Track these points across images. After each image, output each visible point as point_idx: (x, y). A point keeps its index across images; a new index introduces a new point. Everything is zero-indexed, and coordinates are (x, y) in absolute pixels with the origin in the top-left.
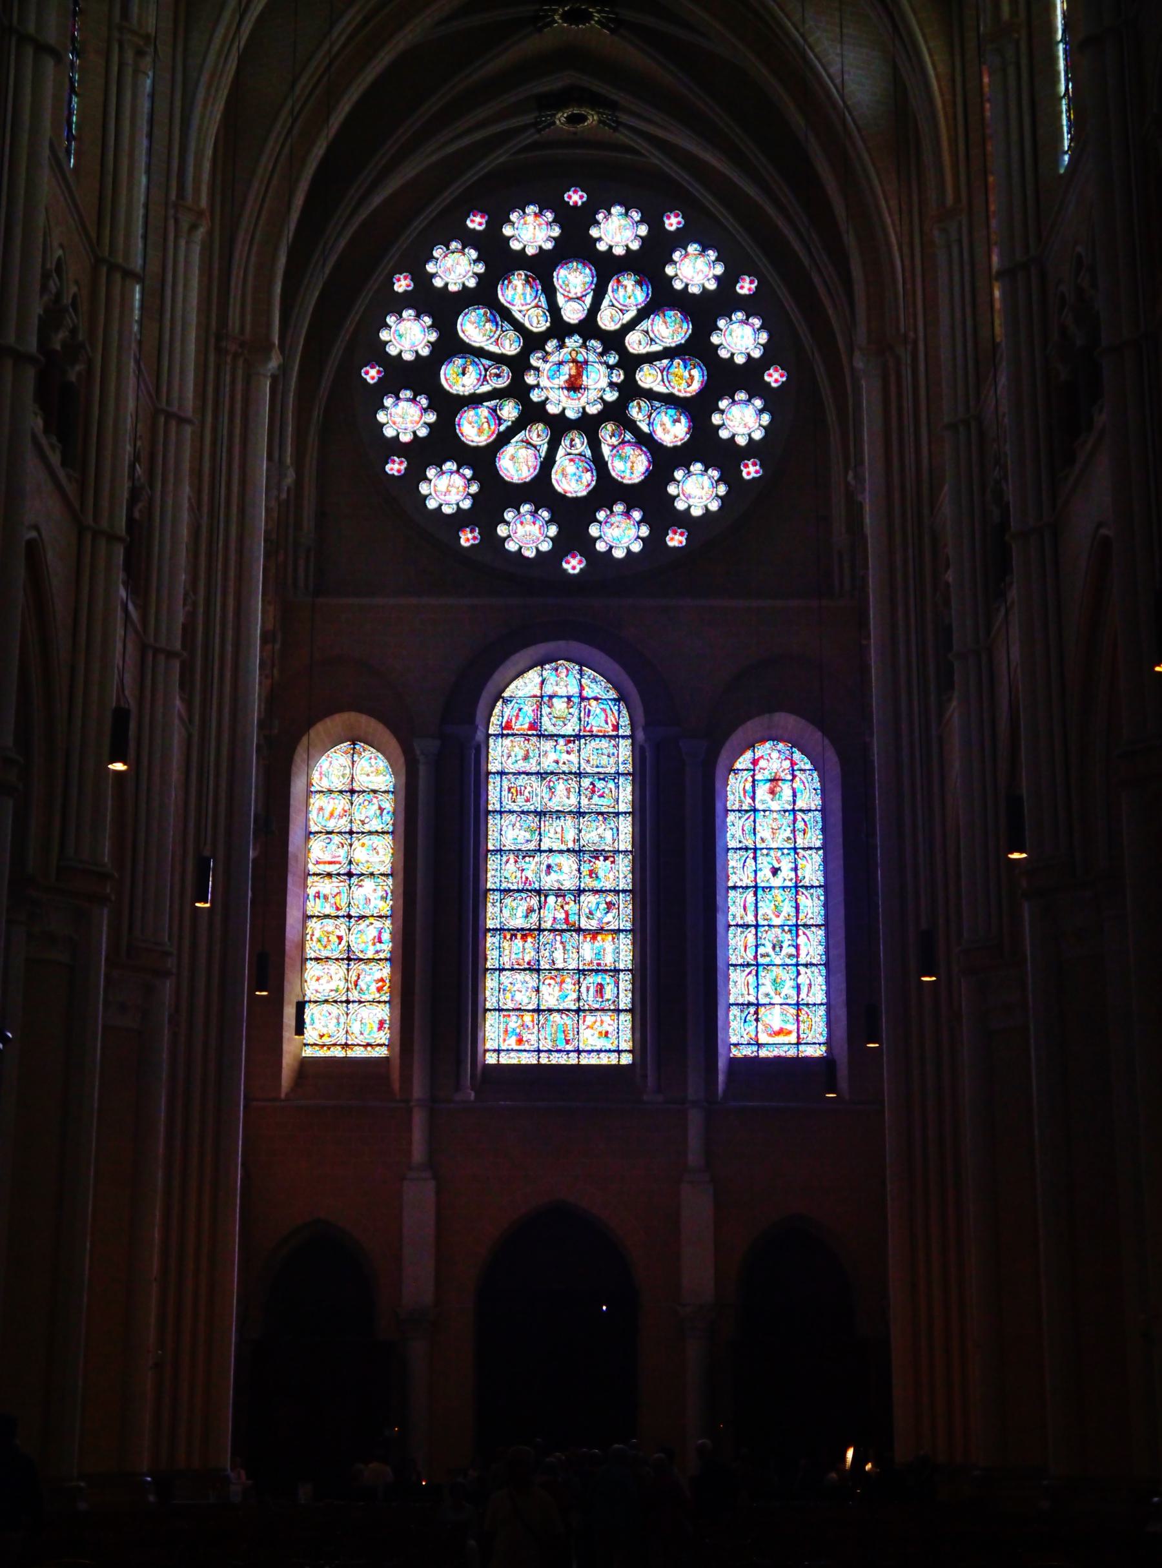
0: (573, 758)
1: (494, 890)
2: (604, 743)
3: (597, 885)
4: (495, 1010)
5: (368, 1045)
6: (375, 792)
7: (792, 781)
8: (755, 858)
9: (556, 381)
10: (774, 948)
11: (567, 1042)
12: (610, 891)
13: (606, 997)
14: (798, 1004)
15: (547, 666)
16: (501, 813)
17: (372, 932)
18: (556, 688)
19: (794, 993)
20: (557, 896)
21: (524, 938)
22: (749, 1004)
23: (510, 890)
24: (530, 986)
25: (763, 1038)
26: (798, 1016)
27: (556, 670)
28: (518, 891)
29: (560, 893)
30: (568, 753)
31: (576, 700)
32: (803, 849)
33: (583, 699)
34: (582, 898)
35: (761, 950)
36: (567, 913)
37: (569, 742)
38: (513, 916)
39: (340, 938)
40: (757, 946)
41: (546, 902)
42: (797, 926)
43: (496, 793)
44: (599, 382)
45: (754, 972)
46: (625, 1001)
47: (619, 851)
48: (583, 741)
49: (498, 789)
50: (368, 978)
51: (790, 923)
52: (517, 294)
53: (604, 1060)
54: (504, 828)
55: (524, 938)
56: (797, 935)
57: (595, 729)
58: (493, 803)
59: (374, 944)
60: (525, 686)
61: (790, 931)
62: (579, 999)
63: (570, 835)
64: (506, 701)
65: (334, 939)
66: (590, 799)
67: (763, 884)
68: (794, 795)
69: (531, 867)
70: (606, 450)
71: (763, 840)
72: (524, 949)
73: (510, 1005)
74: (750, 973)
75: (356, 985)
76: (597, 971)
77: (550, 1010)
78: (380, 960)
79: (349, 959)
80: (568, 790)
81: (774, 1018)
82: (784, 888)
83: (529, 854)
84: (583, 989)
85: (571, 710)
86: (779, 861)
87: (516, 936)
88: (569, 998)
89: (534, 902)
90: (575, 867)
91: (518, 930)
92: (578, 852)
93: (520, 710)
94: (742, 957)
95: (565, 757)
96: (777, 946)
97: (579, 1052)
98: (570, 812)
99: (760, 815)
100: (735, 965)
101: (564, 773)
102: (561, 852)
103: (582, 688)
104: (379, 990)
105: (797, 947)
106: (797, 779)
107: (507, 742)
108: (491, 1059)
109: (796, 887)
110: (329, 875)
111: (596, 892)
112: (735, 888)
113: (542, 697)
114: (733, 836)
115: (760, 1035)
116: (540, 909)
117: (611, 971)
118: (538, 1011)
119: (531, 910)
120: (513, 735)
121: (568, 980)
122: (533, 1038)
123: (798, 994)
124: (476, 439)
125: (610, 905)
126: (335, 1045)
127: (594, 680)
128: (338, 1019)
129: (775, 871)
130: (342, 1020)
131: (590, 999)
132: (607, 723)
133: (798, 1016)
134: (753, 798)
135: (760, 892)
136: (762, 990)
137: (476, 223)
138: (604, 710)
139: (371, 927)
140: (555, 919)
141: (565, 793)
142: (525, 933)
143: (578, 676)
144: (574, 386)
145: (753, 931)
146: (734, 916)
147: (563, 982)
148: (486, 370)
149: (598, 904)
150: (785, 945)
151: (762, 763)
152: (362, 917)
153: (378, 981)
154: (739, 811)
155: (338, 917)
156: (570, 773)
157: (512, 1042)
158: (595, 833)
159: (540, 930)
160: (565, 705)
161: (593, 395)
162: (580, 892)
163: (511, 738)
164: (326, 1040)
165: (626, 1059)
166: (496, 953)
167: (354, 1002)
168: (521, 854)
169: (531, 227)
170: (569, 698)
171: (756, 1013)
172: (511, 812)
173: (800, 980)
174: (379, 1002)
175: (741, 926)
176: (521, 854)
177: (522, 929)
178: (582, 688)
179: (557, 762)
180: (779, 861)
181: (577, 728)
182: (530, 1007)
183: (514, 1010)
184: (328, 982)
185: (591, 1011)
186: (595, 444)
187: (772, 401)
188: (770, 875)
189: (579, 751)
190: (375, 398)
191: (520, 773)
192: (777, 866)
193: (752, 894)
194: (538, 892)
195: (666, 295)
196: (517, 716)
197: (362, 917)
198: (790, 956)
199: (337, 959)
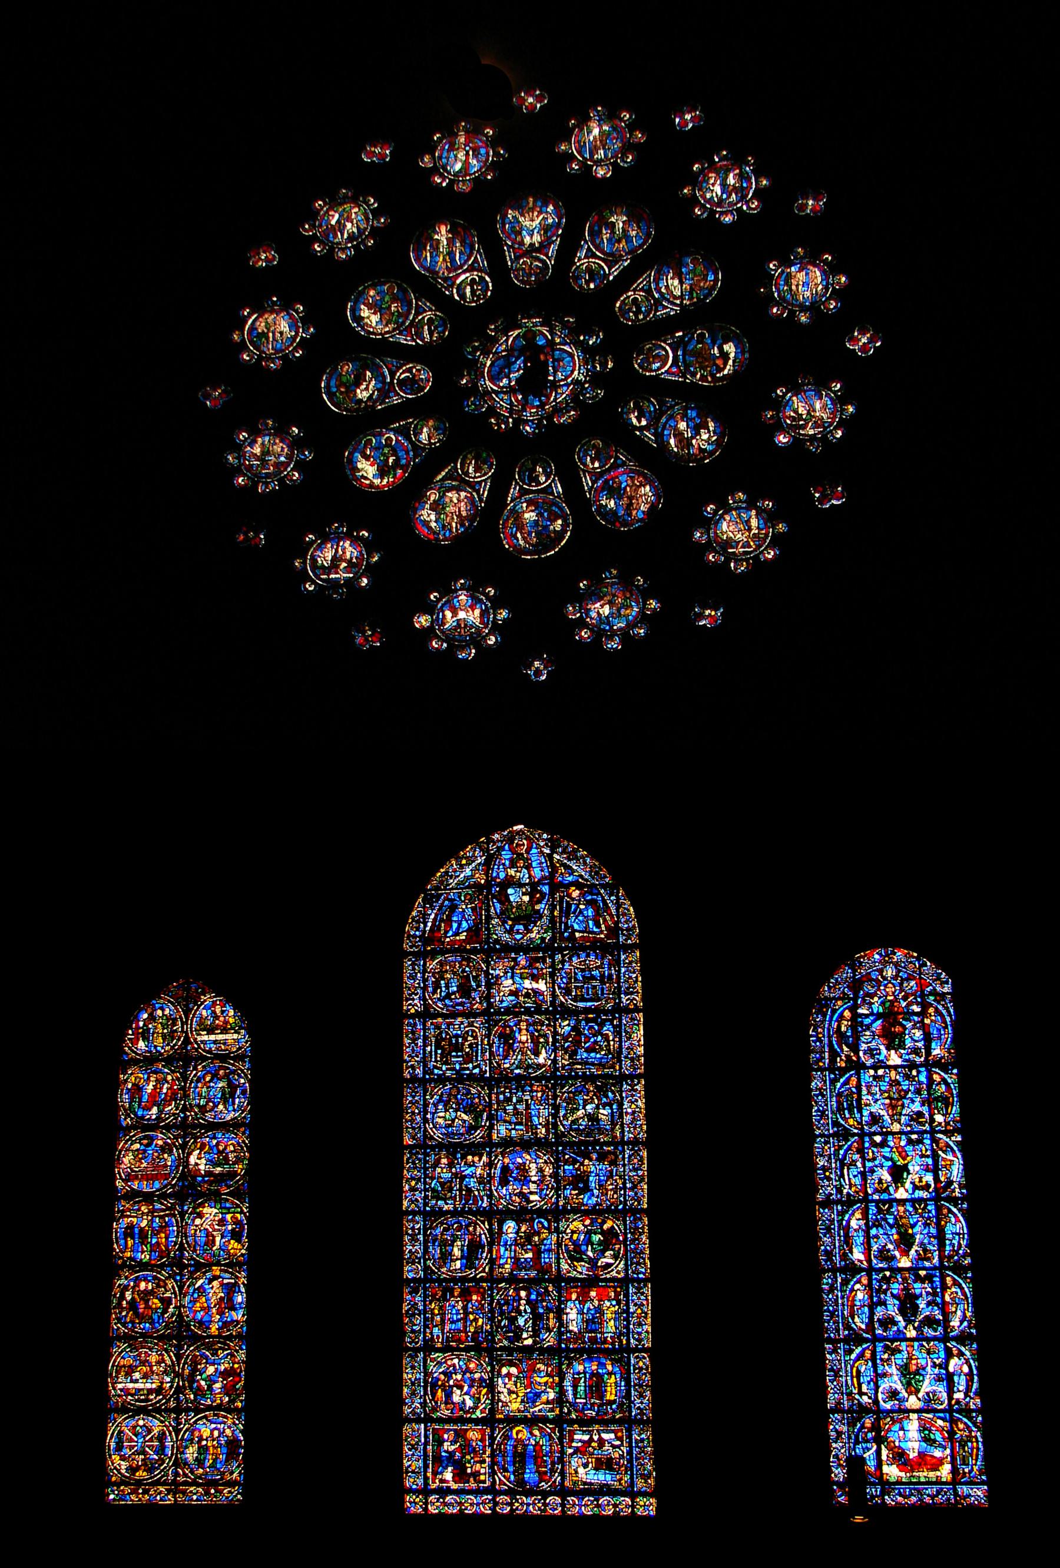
0: (541, 986)
1: (414, 1213)
2: (593, 960)
3: (589, 1201)
4: (418, 1421)
5: (214, 1483)
6: (224, 1058)
7: (923, 1014)
8: (861, 1151)
9: (505, 381)
10: (902, 1311)
11: (542, 1476)
12: (608, 1210)
13: (610, 1397)
14: (950, 1410)
15: (496, 836)
16: (423, 1082)
17: (215, 1292)
18: (511, 872)
19: (941, 1389)
20: (519, 1222)
21: (465, 1295)
22: (863, 1410)
23: (441, 1213)
24: (477, 1376)
25: (892, 1472)
26: (952, 1433)
27: (510, 840)
28: (455, 1213)
29: (521, 1215)
30: (535, 978)
31: (546, 889)
32: (945, 1132)
33: (555, 887)
34: (562, 1225)
35: (879, 1312)
36: (538, 1253)
37: (537, 960)
38: (446, 1257)
39: (166, 1302)
40: (872, 1307)
41: (500, 1232)
42: (941, 1267)
43: (415, 1052)
44: (571, 370)
45: (868, 1354)
46: (642, 1403)
47: (623, 1143)
48: (558, 957)
49: (420, 1042)
50: (211, 1370)
51: (927, 1264)
52: (443, 248)
53: (608, 1506)
54: (431, 1108)
55: (465, 1295)
56: (944, 1287)
57: (577, 935)
58: (412, 1065)
59: (221, 1313)
60: (465, 870)
61: (929, 1278)
62: (561, 1399)
63: (541, 1114)
64: (429, 900)
65: (155, 1302)
66: (575, 1053)
67: (876, 1197)
68: (928, 1039)
69: (476, 1167)
70: (587, 481)
71: (875, 1119)
72: (466, 1313)
73: (445, 1412)
74: (861, 1356)
75: (191, 1379)
76: (590, 1352)
77: (512, 1421)
78: (230, 1337)
79: (180, 1338)
80: (535, 1041)
81: (910, 1437)
82: (913, 1201)
83: (475, 1149)
84: (567, 1383)
85: (537, 907)
86: (904, 1155)
87: (452, 1291)
88: (544, 1398)
89: (482, 1230)
90: (548, 1170)
91: (454, 1280)
92: (553, 1145)
93: (453, 908)
94: (847, 1327)
95: (527, 984)
96: (908, 1304)
97: (563, 1492)
98: (538, 1079)
99: (867, 1076)
100: (834, 1342)
101: (528, 1012)
102: (525, 1145)
103: (554, 869)
104: (227, 1390)
105: (944, 1307)
106: (931, 1010)
107: (432, 965)
108: (413, 1504)
109: (937, 1199)
110: (148, 1198)
111: (586, 1213)
112: (828, 1203)
113: (489, 885)
114: (823, 1114)
115: (886, 1469)
116: (491, 1244)
117: (614, 1351)
118: (490, 1421)
119: (473, 1249)
120: (443, 952)
121: (542, 1367)
122: (483, 1469)
123: (950, 1392)
124: (377, 482)
125: (610, 1236)
126: (158, 1483)
127: (573, 856)
128: (161, 1437)
129: (898, 1173)
130: (169, 1444)
131: (577, 1395)
132: (598, 925)
133: (952, 1433)
134: (855, 1048)
135: (873, 1209)
136: (884, 1385)
137: (379, 153)
138: (591, 903)
139: (215, 1283)
140: (516, 1260)
141: (530, 1045)
142: (467, 1287)
143: (547, 851)
144: (535, 382)
145: (865, 1281)
146: (829, 1254)
147: (533, 1370)
148: (392, 374)
149: (589, 1233)
150: (922, 1304)
151: (869, 988)
152: (198, 1266)
153: (225, 1374)
154: (832, 1068)
155: (162, 1266)
156: (538, 1011)
157: (448, 1475)
158: (580, 1113)
159: (493, 1279)
160: (526, 898)
161: (563, 394)
162: (556, 1214)
163: (440, 958)
164: (141, 1474)
165: (647, 1507)
166: (419, 1320)
167: (187, 1410)
168: (457, 1149)
169: (461, 155)
170: (534, 885)
171: (876, 1427)
172: (442, 1080)
173: (954, 1364)
174: (229, 1411)
175: (842, 1270)
176: (457, 1149)
177: (464, 1279)
178: (554, 869)
179: (514, 993)
180: (904, 1155)
181: (548, 936)
182: (478, 1414)
183: (449, 1420)
184: (145, 1376)
185: (585, 1423)
186: (570, 477)
187: (858, 380)
188: (887, 1177)
189: (552, 975)
190: (221, 431)
191: (454, 1015)
192: (901, 1162)
193: (858, 1215)
194: (489, 1214)
195: (678, 235)
196: (449, 922)
197: (198, 1266)
198: (929, 1321)
199: (161, 1338)
